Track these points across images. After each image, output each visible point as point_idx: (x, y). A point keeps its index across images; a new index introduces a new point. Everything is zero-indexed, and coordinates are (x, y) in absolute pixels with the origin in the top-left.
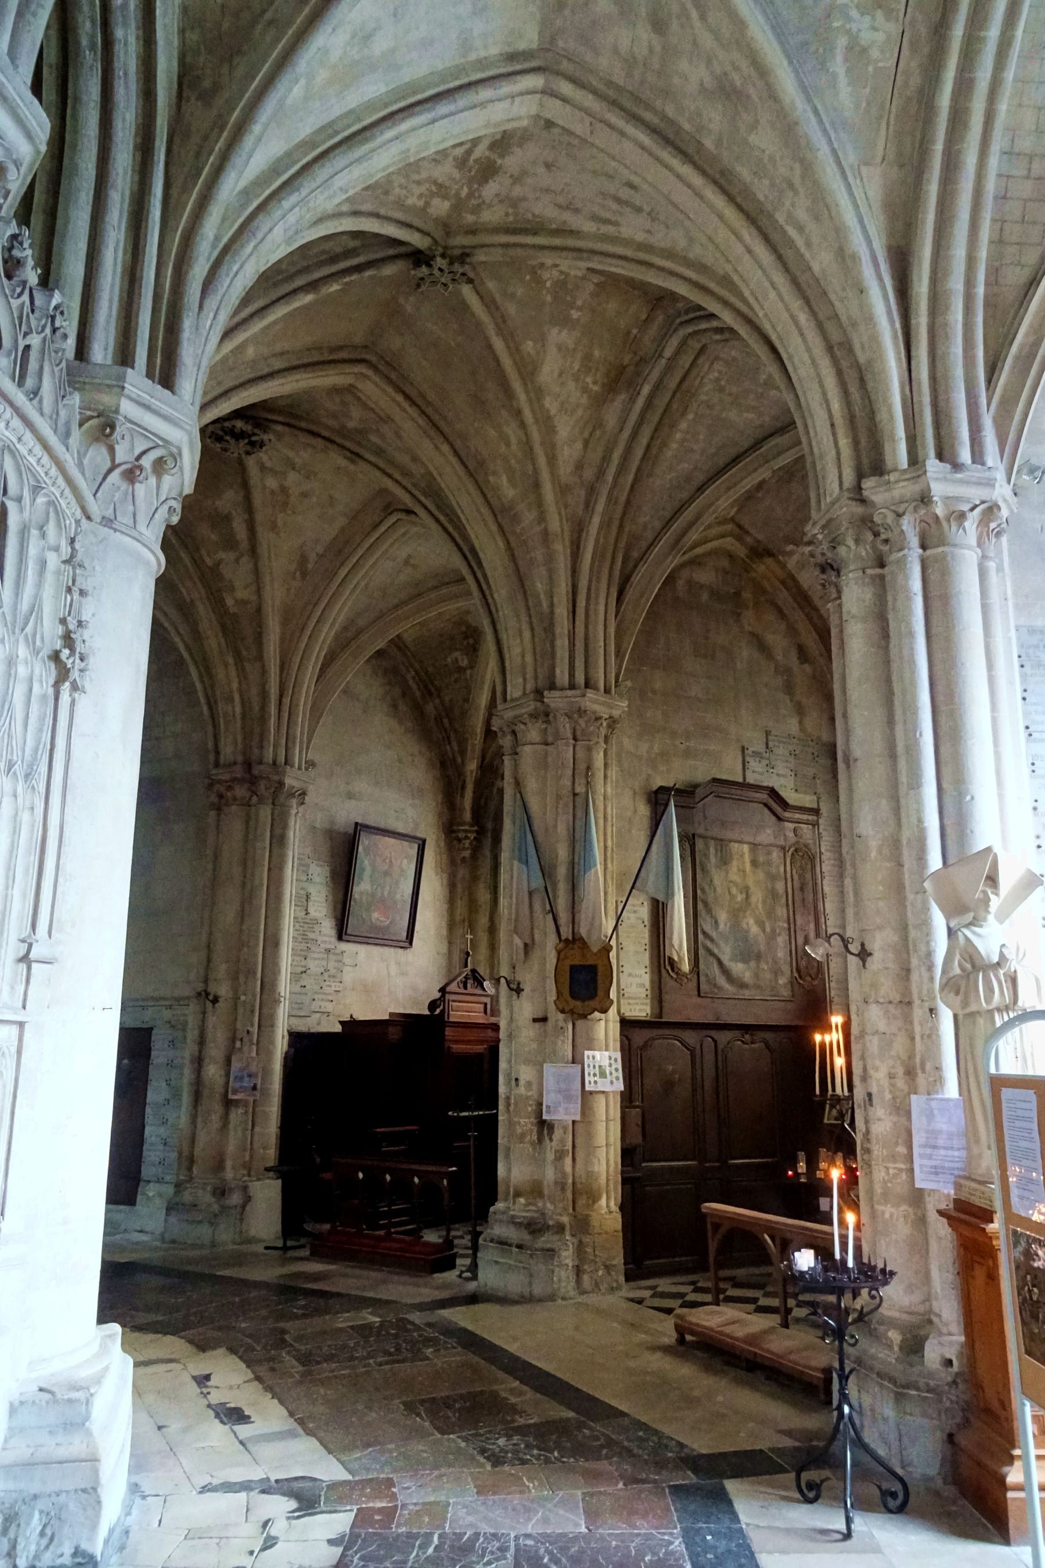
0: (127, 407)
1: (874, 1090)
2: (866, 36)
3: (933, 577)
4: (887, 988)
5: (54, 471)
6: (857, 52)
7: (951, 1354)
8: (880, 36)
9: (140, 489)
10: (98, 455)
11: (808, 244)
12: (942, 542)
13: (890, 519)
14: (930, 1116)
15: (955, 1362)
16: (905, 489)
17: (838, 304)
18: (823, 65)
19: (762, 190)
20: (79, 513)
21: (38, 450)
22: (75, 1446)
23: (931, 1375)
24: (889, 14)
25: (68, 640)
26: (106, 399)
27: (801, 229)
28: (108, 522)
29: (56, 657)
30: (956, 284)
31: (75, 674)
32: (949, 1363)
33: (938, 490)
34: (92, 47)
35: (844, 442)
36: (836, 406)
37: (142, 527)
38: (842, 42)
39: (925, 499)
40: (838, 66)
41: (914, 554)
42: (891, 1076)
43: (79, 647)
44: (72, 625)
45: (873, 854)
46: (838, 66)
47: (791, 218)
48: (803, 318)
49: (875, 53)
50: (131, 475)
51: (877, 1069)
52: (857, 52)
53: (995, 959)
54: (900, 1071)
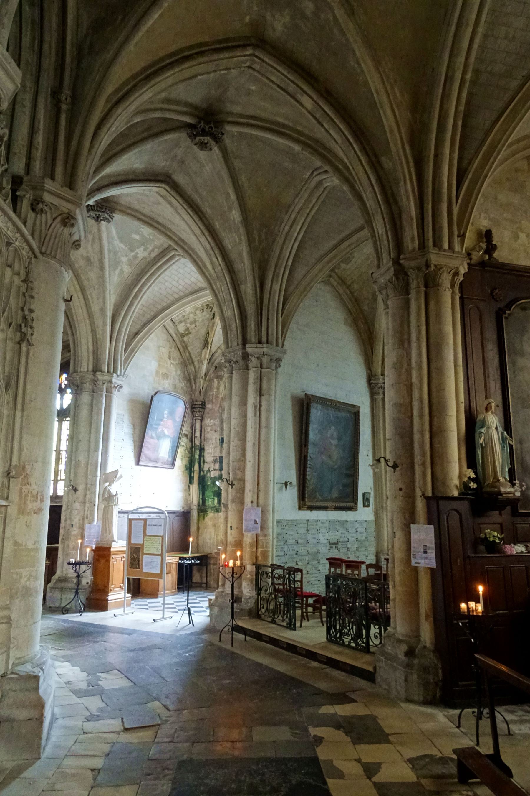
1: (74, 523)
2: (125, 269)
3: (107, 400)
4: (81, 499)
6: (122, 272)
7: (89, 581)
8: (127, 271)
11: (93, 302)
12: (111, 393)
13: (101, 383)
14: (90, 529)
15: (89, 583)
16: (106, 378)
17: (95, 321)
18: (115, 270)
19: (85, 283)
23: (84, 586)
24: (131, 267)
27: (92, 298)
30: (124, 330)
32: (88, 583)
33: (114, 380)
35: (91, 358)
36: (91, 348)
38: (120, 268)
39: (110, 382)
40: (117, 272)
41: (105, 394)
42: (79, 520)
45: (83, 465)
46: (117, 272)
47: (91, 294)
48: (88, 321)
49: (125, 273)
51: (75, 518)
52: (122, 272)
53: (114, 494)
54: (81, 519)
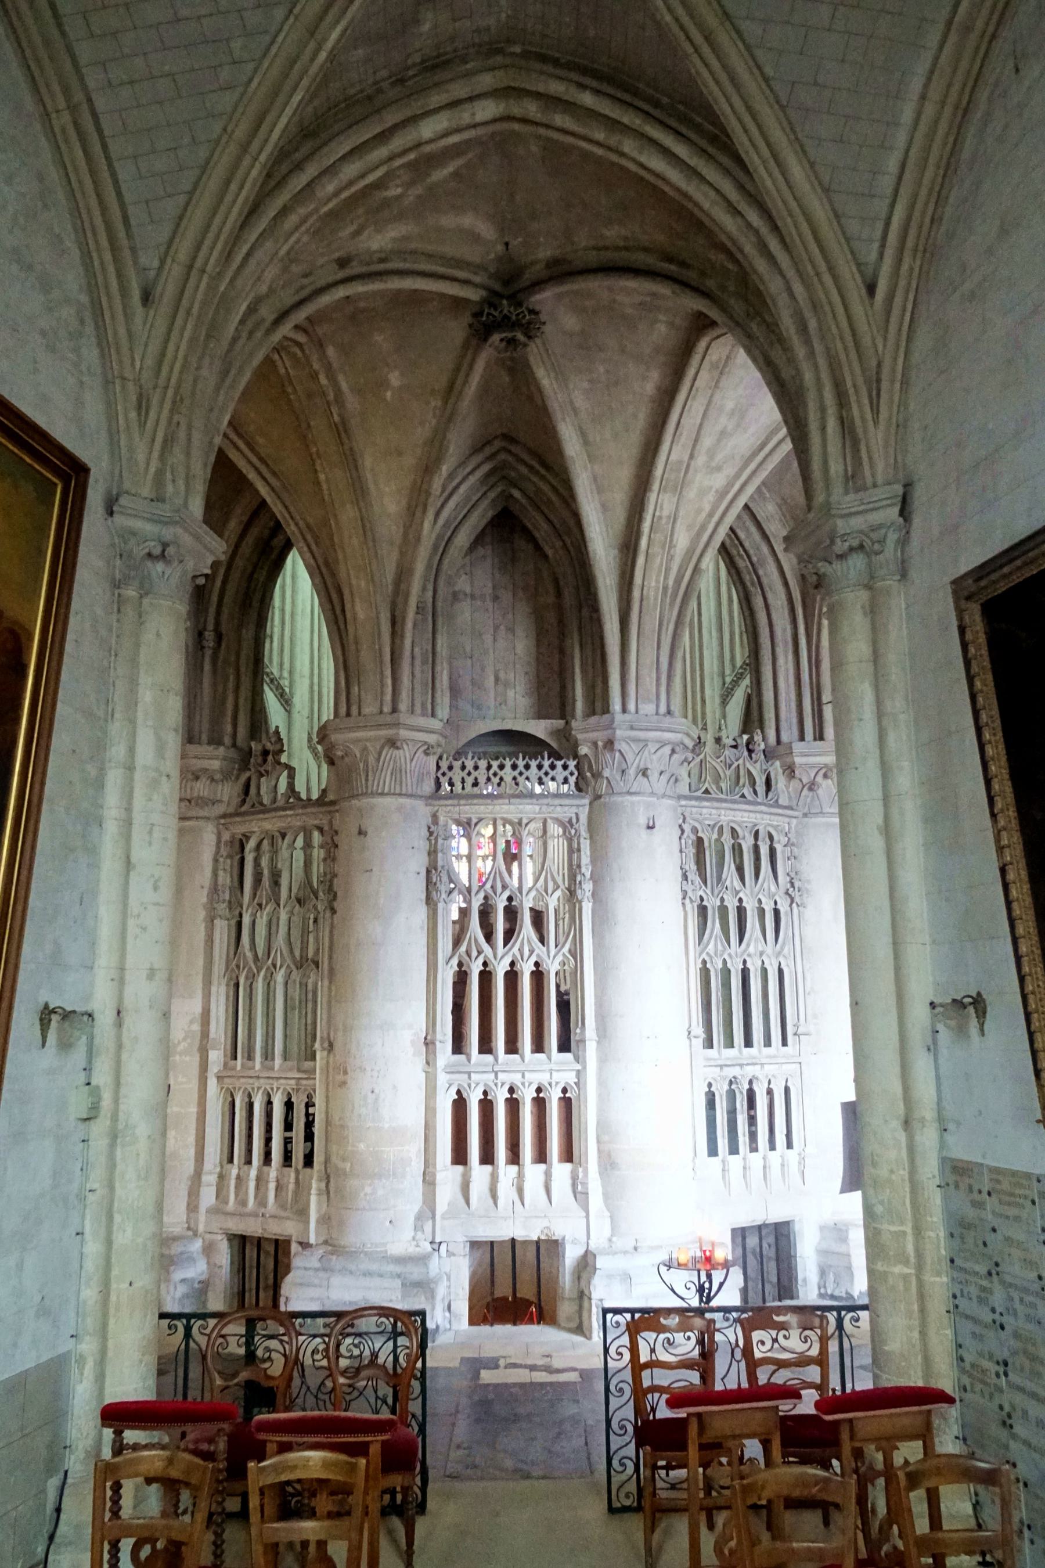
0: (798, 760)
5: (758, 816)
9: (820, 792)
10: (795, 784)
20: (787, 820)
21: (746, 814)
22: (842, 1249)
25: (792, 885)
26: (788, 760)
28: (805, 815)
29: (787, 893)
31: (797, 899)
34: (753, 584)
37: (827, 810)
43: (797, 884)
44: (793, 875)
50: (812, 786)
